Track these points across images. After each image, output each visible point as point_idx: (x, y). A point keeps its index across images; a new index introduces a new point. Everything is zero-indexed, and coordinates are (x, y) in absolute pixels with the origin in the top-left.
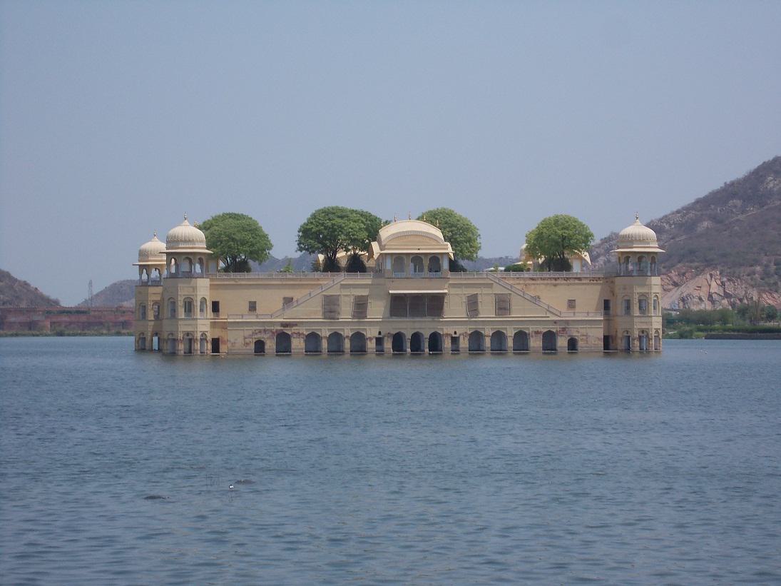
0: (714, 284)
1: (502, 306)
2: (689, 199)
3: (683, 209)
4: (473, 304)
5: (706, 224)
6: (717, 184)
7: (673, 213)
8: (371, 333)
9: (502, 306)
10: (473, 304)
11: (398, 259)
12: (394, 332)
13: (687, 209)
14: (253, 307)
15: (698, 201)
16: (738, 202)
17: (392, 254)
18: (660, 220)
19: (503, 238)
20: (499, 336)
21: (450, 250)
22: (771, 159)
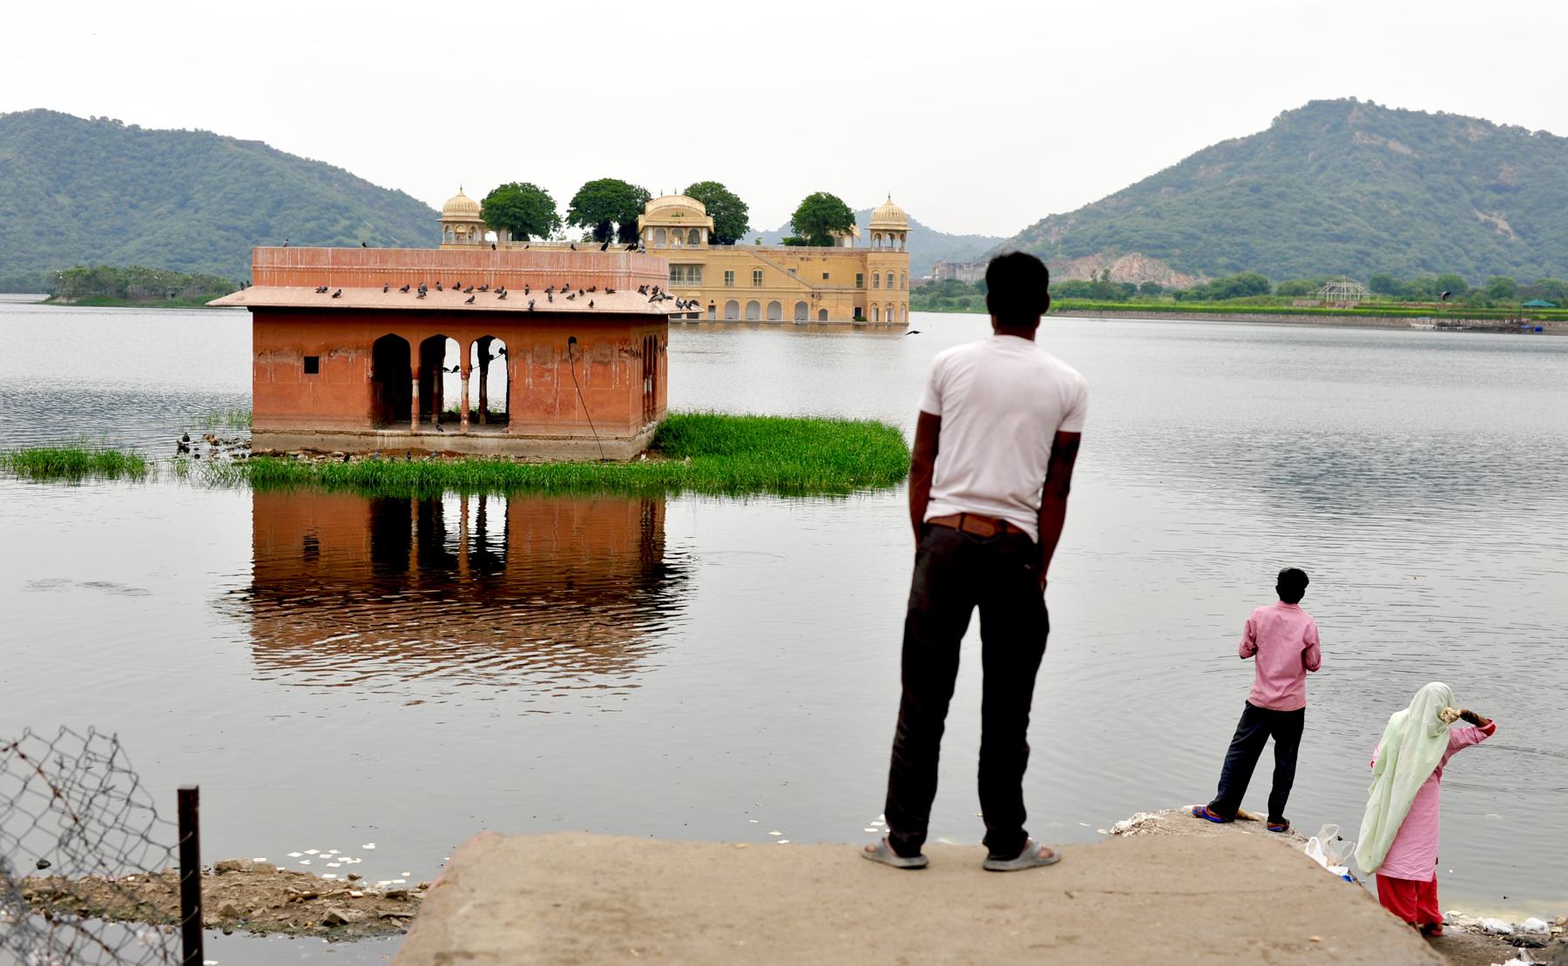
0: (1136, 265)
1: (757, 277)
2: (1125, 185)
4: (729, 276)
7: (1109, 197)
9: (757, 277)
10: (729, 276)
11: (660, 230)
15: (1134, 186)
19: (770, 215)
20: (754, 304)
21: (710, 222)
22: (1202, 147)
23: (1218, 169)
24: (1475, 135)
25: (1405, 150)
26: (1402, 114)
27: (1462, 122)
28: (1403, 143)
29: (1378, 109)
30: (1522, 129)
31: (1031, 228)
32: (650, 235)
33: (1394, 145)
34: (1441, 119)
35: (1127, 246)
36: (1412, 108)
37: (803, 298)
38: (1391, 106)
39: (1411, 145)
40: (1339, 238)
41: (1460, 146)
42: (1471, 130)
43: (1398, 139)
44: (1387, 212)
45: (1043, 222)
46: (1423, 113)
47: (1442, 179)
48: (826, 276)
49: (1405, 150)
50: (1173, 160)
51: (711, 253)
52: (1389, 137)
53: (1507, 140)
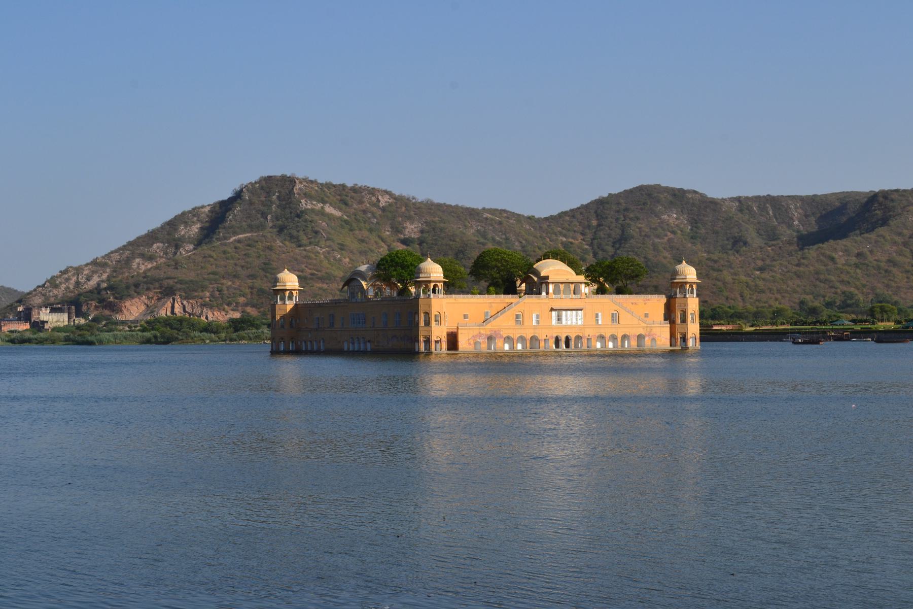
0: (176, 305)
1: (615, 318)
3: (119, 249)
5: (137, 260)
6: (143, 232)
7: (112, 252)
8: (542, 337)
9: (615, 318)
11: (556, 284)
12: (555, 335)
13: (124, 248)
14: (466, 317)
15: (130, 244)
16: (161, 245)
17: (553, 283)
18: (103, 257)
23: (195, 229)
24: (384, 201)
25: (337, 213)
26: (329, 186)
27: (373, 192)
28: (335, 208)
29: (312, 182)
30: (414, 198)
31: (53, 278)
32: (551, 287)
33: (329, 209)
34: (355, 190)
35: (168, 292)
36: (336, 182)
37: (641, 331)
38: (322, 180)
39: (340, 210)
40: (322, 279)
41: (374, 209)
42: (380, 198)
43: (331, 205)
44: (340, 260)
45: (66, 272)
46: (343, 186)
47: (366, 233)
48: (646, 315)
49: (337, 213)
50: (156, 221)
51: (587, 300)
52: (324, 202)
53: (406, 205)
